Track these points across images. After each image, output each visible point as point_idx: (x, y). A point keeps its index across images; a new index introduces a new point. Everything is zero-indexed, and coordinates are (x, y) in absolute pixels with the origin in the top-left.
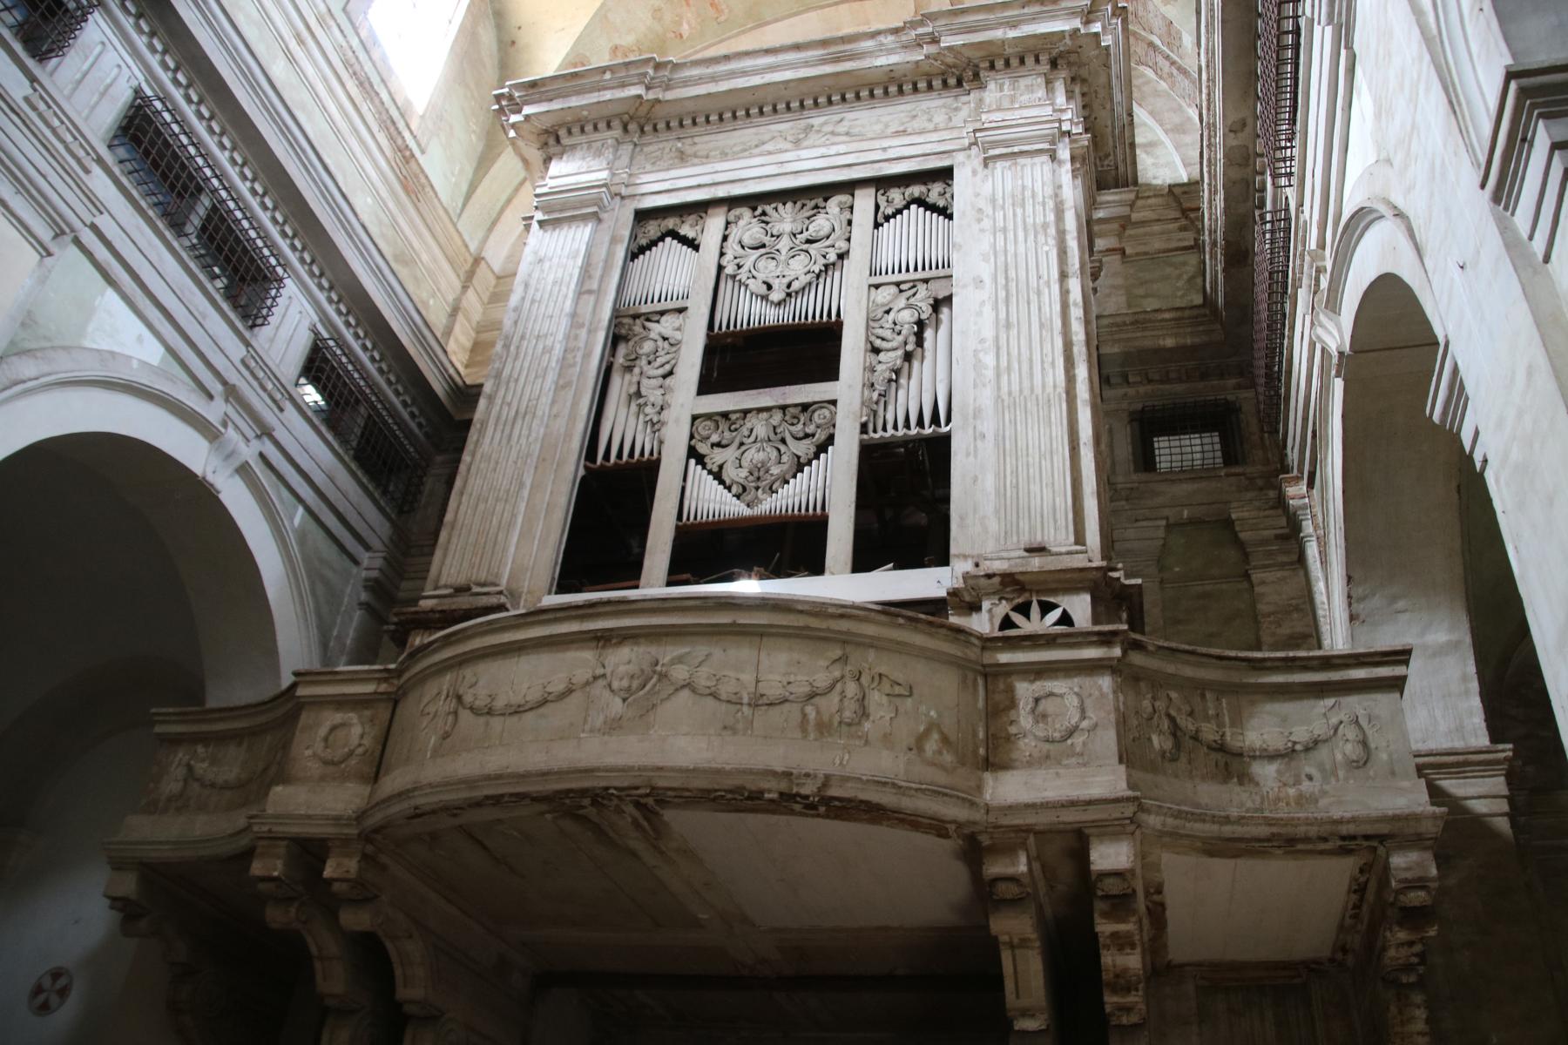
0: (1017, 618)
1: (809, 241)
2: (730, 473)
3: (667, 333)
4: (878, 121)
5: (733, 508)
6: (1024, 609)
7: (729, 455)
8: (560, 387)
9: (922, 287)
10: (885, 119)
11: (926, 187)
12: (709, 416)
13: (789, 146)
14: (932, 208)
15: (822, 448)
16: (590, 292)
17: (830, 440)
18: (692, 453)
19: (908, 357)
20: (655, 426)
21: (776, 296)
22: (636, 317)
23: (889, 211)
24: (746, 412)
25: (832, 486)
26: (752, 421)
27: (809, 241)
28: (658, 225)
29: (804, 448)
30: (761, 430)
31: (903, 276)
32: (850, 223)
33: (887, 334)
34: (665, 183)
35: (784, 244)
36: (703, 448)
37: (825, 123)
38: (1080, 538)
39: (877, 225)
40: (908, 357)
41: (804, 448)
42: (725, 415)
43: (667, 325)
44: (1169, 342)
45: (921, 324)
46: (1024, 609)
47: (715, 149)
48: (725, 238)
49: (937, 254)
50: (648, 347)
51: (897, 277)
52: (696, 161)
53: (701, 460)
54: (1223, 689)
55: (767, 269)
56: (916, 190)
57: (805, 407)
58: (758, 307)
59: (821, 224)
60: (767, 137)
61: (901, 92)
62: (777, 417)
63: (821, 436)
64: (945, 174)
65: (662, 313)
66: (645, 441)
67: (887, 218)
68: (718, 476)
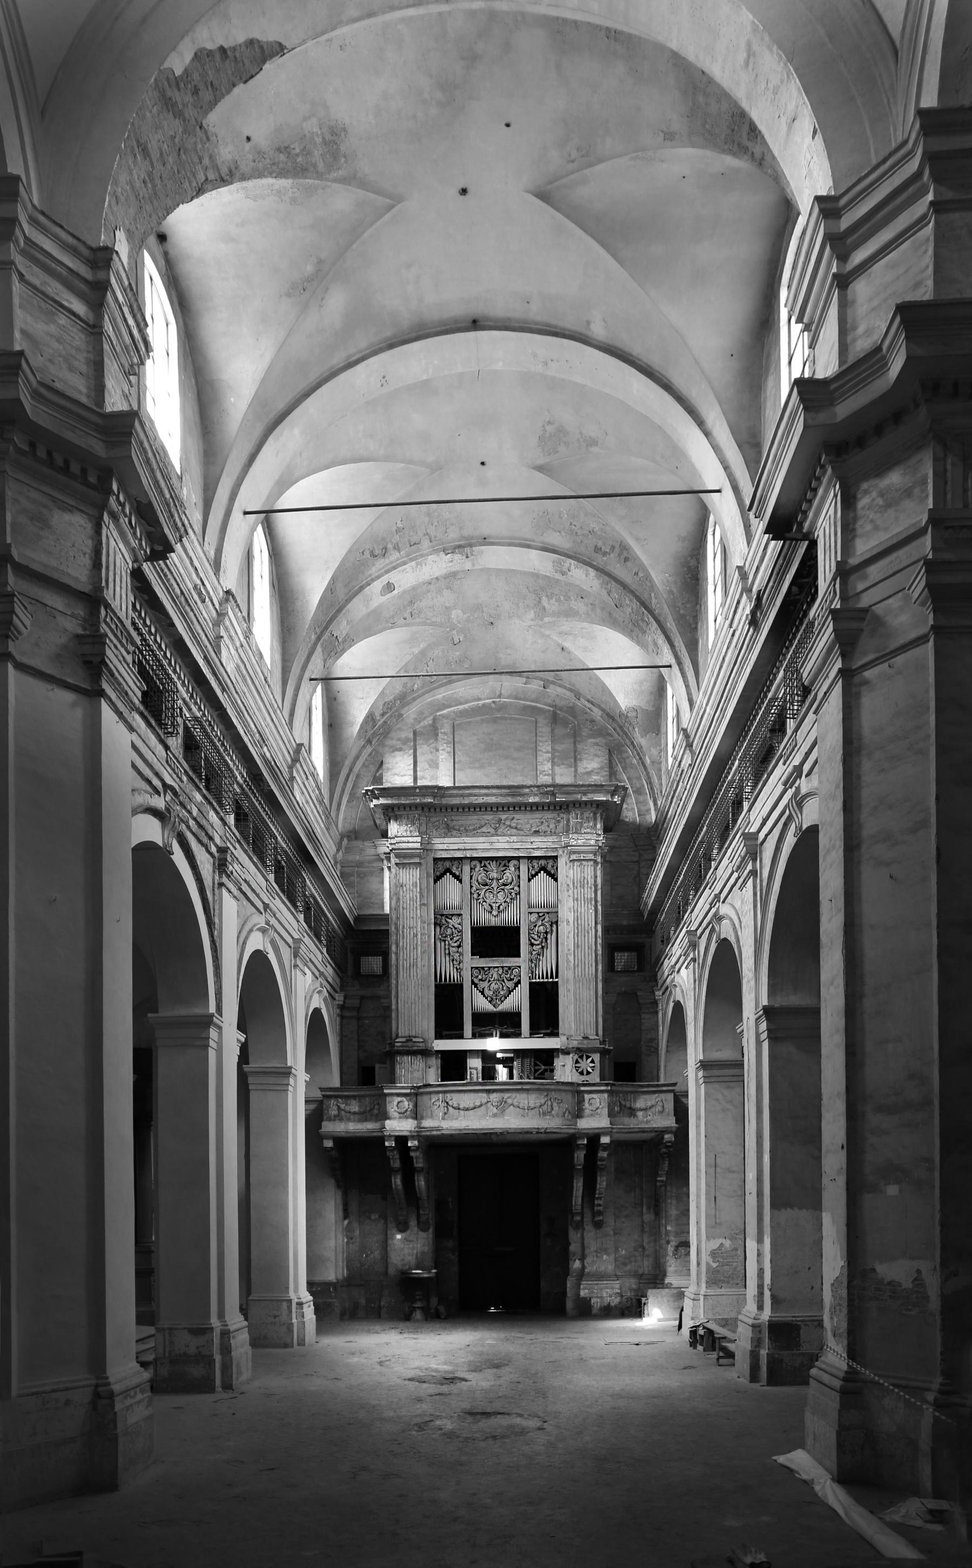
0: (580, 1060)
1: (504, 885)
2: (487, 992)
3: (456, 926)
4: (528, 823)
5: (489, 1007)
6: (581, 1057)
7: (485, 984)
8: (423, 953)
9: (547, 916)
10: (531, 822)
11: (546, 866)
12: (477, 968)
13: (492, 831)
14: (549, 874)
15: (516, 985)
16: (424, 904)
17: (519, 982)
18: (473, 983)
19: (543, 947)
20: (459, 970)
21: (495, 913)
22: (442, 915)
23: (533, 873)
24: (490, 968)
25: (519, 1000)
26: (492, 971)
27: (504, 885)
28: (445, 868)
29: (510, 985)
30: (495, 976)
31: (540, 910)
32: (519, 877)
33: (536, 937)
34: (447, 846)
35: (494, 884)
36: (476, 981)
37: (506, 819)
38: (597, 1035)
39: (529, 880)
40: (543, 947)
41: (510, 985)
42: (483, 968)
43: (454, 922)
44: (625, 923)
45: (546, 933)
46: (581, 1057)
47: (462, 826)
48: (471, 877)
49: (552, 899)
50: (449, 931)
51: (537, 910)
52: (454, 833)
53: (476, 986)
54: (632, 1092)
55: (490, 898)
56: (543, 862)
57: (509, 968)
58: (487, 915)
59: (509, 875)
60: (483, 823)
61: (537, 809)
62: (501, 971)
63: (516, 980)
64: (555, 858)
65: (452, 915)
66: (454, 974)
67: (533, 876)
68: (482, 993)
